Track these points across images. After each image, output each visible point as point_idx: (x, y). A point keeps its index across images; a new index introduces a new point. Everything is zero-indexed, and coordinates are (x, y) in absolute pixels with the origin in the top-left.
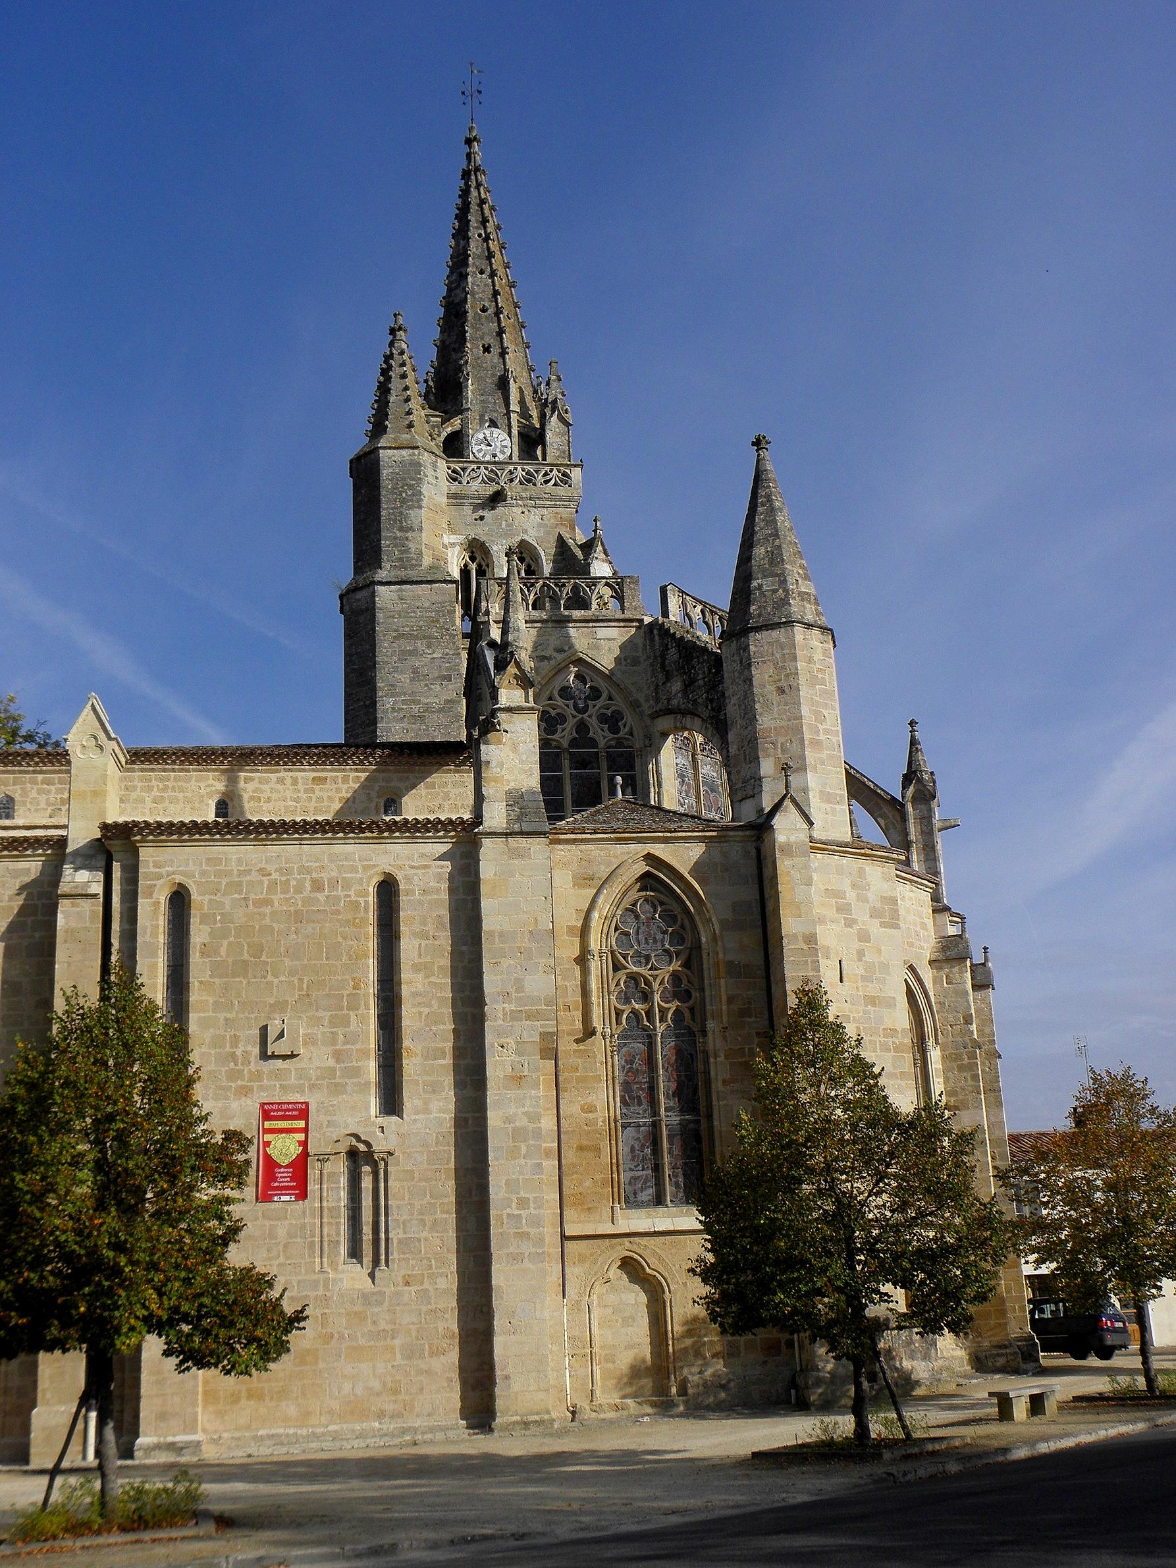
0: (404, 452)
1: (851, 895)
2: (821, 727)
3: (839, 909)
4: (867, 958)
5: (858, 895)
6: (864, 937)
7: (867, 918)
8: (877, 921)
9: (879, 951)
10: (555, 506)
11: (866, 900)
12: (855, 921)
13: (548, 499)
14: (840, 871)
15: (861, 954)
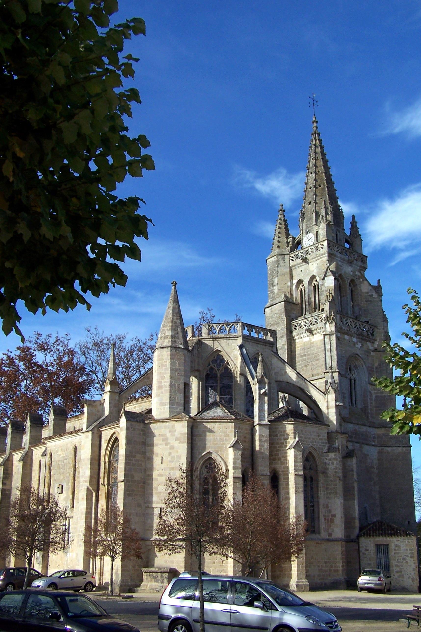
0: (273, 258)
1: (168, 435)
2: (163, 381)
3: (164, 440)
4: (173, 454)
5: (171, 434)
6: (172, 448)
7: (174, 441)
8: (178, 442)
9: (177, 452)
10: (321, 258)
11: (174, 435)
12: (169, 443)
13: (318, 256)
14: (165, 427)
15: (170, 454)
